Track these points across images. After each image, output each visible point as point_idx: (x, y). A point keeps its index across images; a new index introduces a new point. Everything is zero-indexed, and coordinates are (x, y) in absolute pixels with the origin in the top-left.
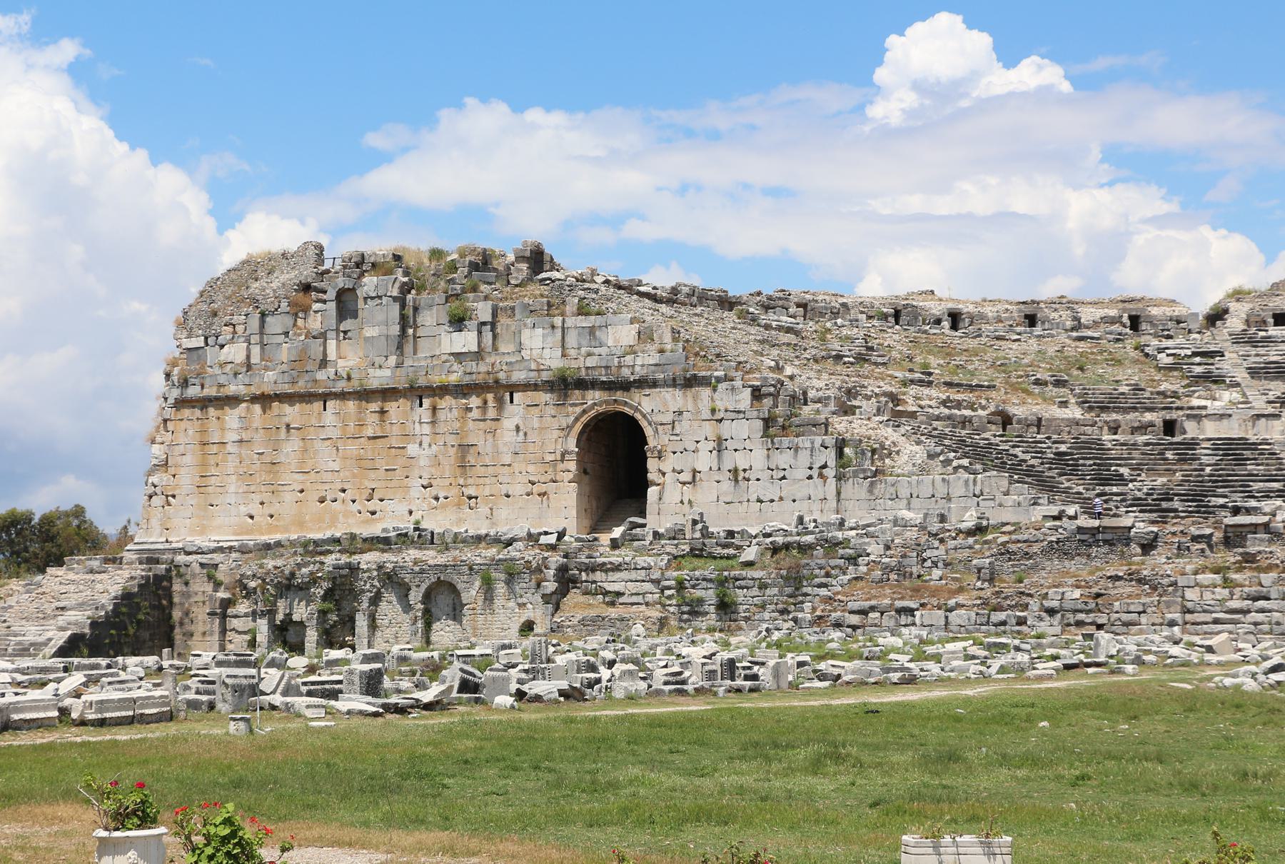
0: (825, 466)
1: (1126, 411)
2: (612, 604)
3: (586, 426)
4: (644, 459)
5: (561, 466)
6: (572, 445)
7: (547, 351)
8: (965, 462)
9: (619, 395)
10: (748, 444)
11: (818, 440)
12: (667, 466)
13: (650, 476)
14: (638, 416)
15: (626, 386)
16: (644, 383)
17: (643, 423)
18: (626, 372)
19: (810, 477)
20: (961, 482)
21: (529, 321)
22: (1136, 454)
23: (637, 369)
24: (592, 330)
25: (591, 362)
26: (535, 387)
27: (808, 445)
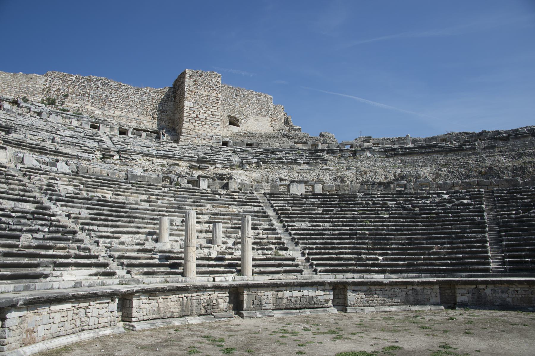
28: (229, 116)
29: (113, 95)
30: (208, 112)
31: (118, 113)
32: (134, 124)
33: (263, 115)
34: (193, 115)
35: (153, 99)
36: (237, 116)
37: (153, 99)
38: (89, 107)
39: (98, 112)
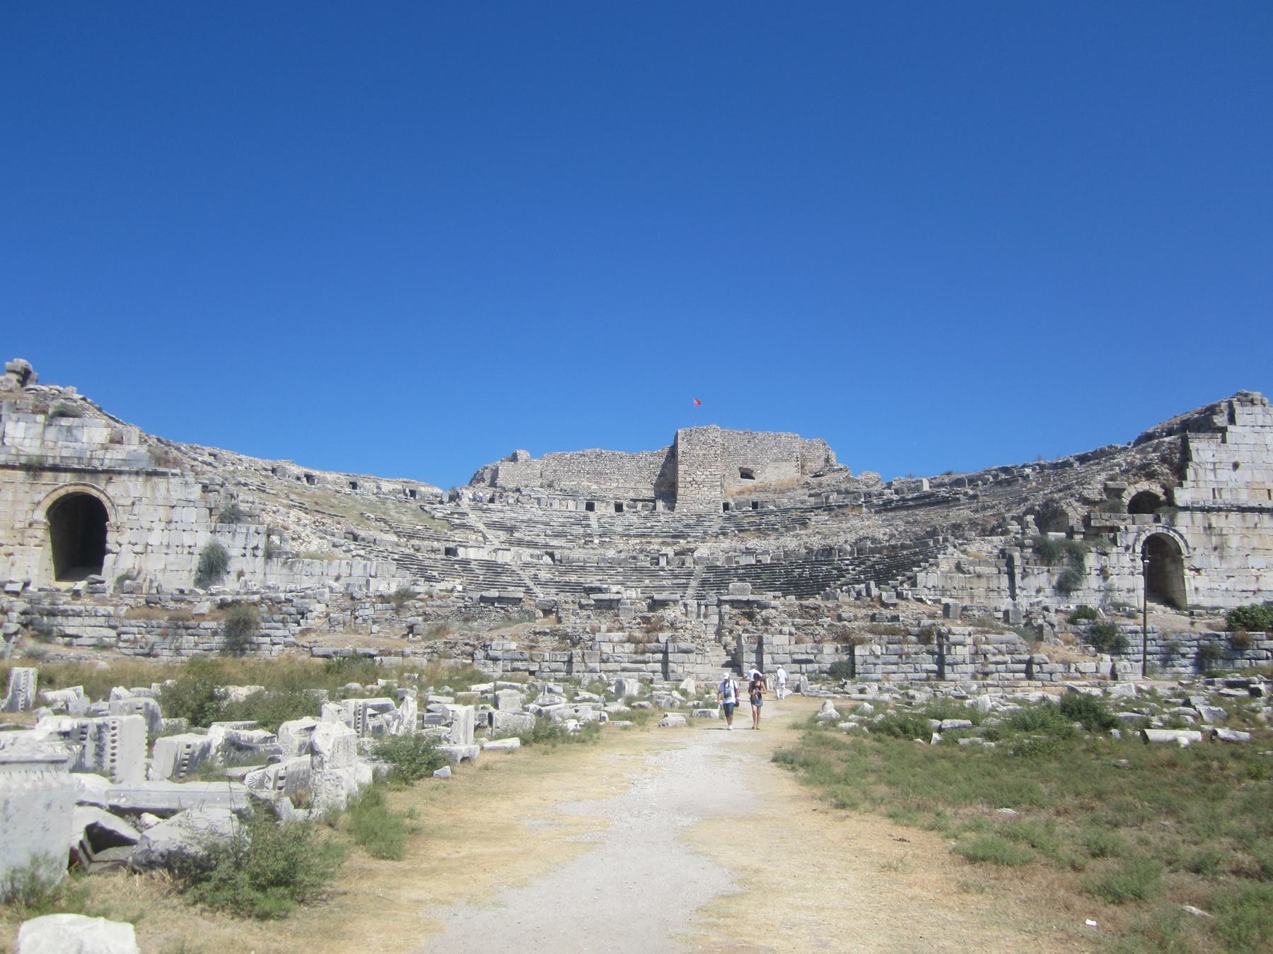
0: (256, 548)
1: (423, 539)
2: (69, 645)
3: (55, 503)
4: (104, 532)
5: (30, 532)
6: (41, 515)
7: (27, 442)
8: (362, 553)
9: (88, 479)
10: (195, 527)
11: (253, 528)
12: (124, 539)
13: (108, 546)
14: (103, 498)
15: (94, 472)
16: (111, 473)
17: (107, 504)
18: (96, 463)
19: (244, 555)
20: (361, 566)
21: (14, 416)
22: (438, 564)
23: (107, 462)
24: (69, 429)
25: (65, 453)
26: (14, 468)
27: (244, 530)
28: (740, 469)
32: (632, 495)
34: (689, 479)
35: (650, 463)
36: (750, 466)
37: (650, 463)
38: (585, 483)
39: (594, 487)
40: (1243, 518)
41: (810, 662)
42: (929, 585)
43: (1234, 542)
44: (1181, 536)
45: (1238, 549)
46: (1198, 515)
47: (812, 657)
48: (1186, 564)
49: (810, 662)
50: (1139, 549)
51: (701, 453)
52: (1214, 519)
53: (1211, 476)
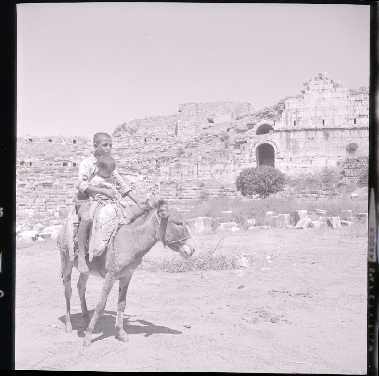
29: (155, 123)
30: (188, 123)
31: (158, 130)
33: (227, 113)
37: (171, 120)
40: (307, 134)
41: (24, 205)
42: (165, 171)
43: (301, 145)
44: (274, 144)
45: (303, 148)
46: (284, 134)
47: (24, 203)
48: (276, 156)
49: (24, 205)
50: (254, 150)
51: (187, 114)
52: (292, 135)
53: (294, 116)
